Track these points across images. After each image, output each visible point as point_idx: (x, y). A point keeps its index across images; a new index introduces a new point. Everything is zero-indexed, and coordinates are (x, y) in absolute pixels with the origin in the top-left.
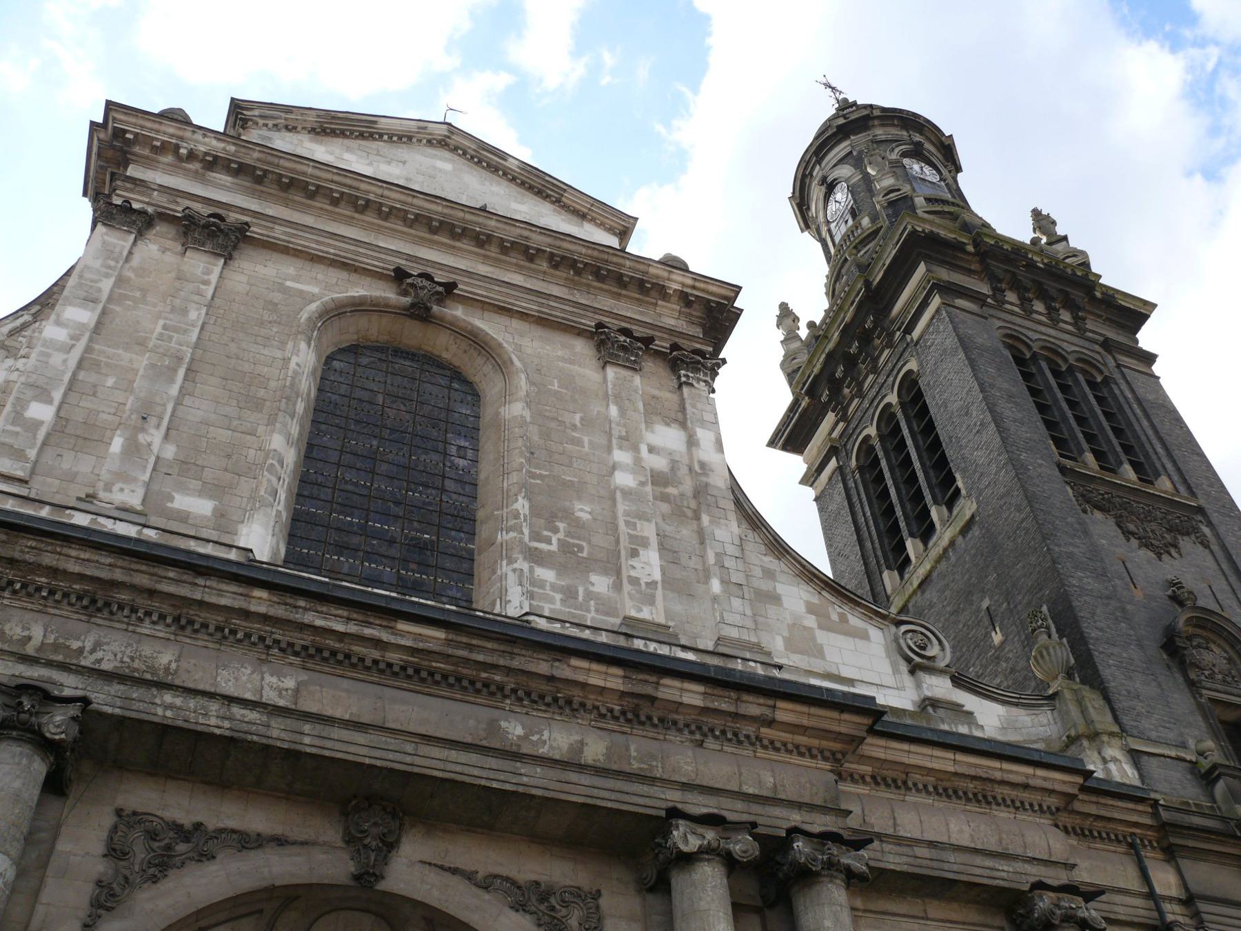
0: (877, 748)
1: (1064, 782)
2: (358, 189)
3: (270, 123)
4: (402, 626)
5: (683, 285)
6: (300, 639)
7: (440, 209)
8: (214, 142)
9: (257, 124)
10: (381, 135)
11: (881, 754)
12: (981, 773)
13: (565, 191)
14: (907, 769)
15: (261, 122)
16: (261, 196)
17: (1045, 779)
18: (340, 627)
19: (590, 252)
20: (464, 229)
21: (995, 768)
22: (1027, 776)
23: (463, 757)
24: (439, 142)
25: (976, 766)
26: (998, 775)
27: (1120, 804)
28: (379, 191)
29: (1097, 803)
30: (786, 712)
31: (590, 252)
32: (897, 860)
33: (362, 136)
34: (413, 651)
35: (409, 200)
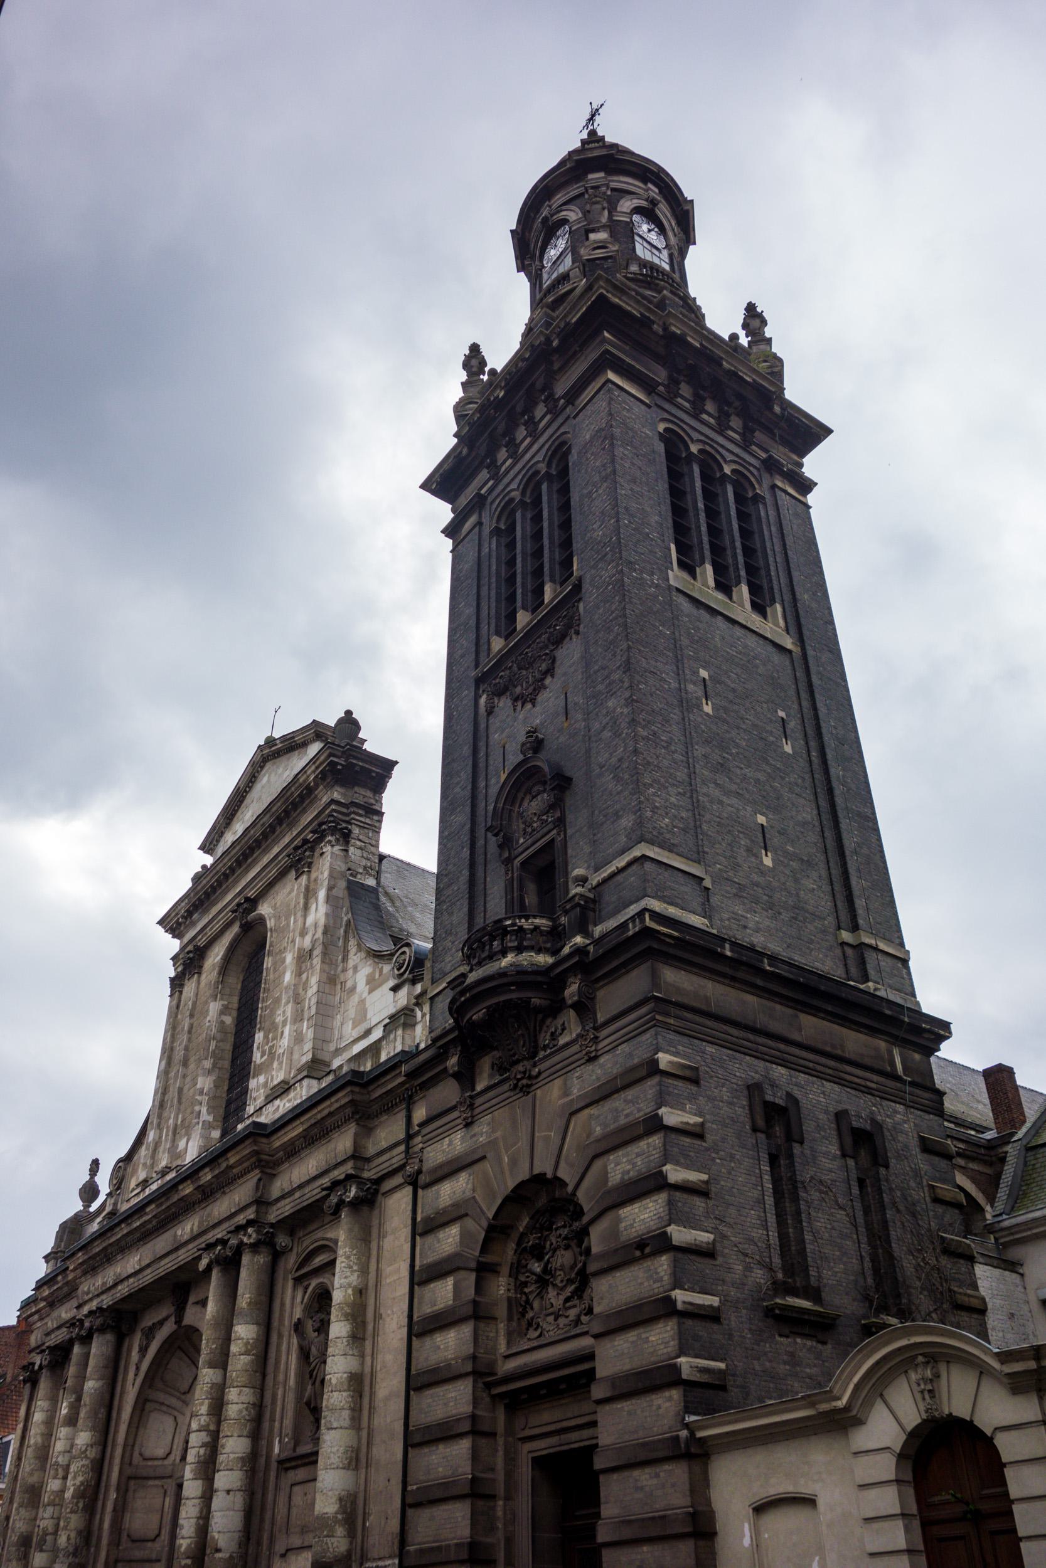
0: (278, 1141)
1: (344, 1096)
2: (218, 872)
3: (215, 842)
4: (148, 1210)
5: (314, 772)
6: (138, 1235)
7: (238, 848)
8: (183, 904)
9: (211, 849)
10: (245, 791)
11: (277, 1144)
12: (313, 1121)
13: (293, 737)
14: (292, 1142)
15: (212, 846)
16: (214, 904)
17: (337, 1101)
18: (138, 1224)
19: (281, 802)
20: (249, 847)
21: (316, 1114)
22: (329, 1106)
23: (166, 1260)
24: (263, 761)
25: (310, 1118)
26: (319, 1117)
27: (388, 1077)
28: (221, 865)
29: (379, 1086)
30: (233, 1159)
31: (281, 802)
32: (288, 1208)
33: (241, 802)
34: (154, 1216)
35: (230, 856)
